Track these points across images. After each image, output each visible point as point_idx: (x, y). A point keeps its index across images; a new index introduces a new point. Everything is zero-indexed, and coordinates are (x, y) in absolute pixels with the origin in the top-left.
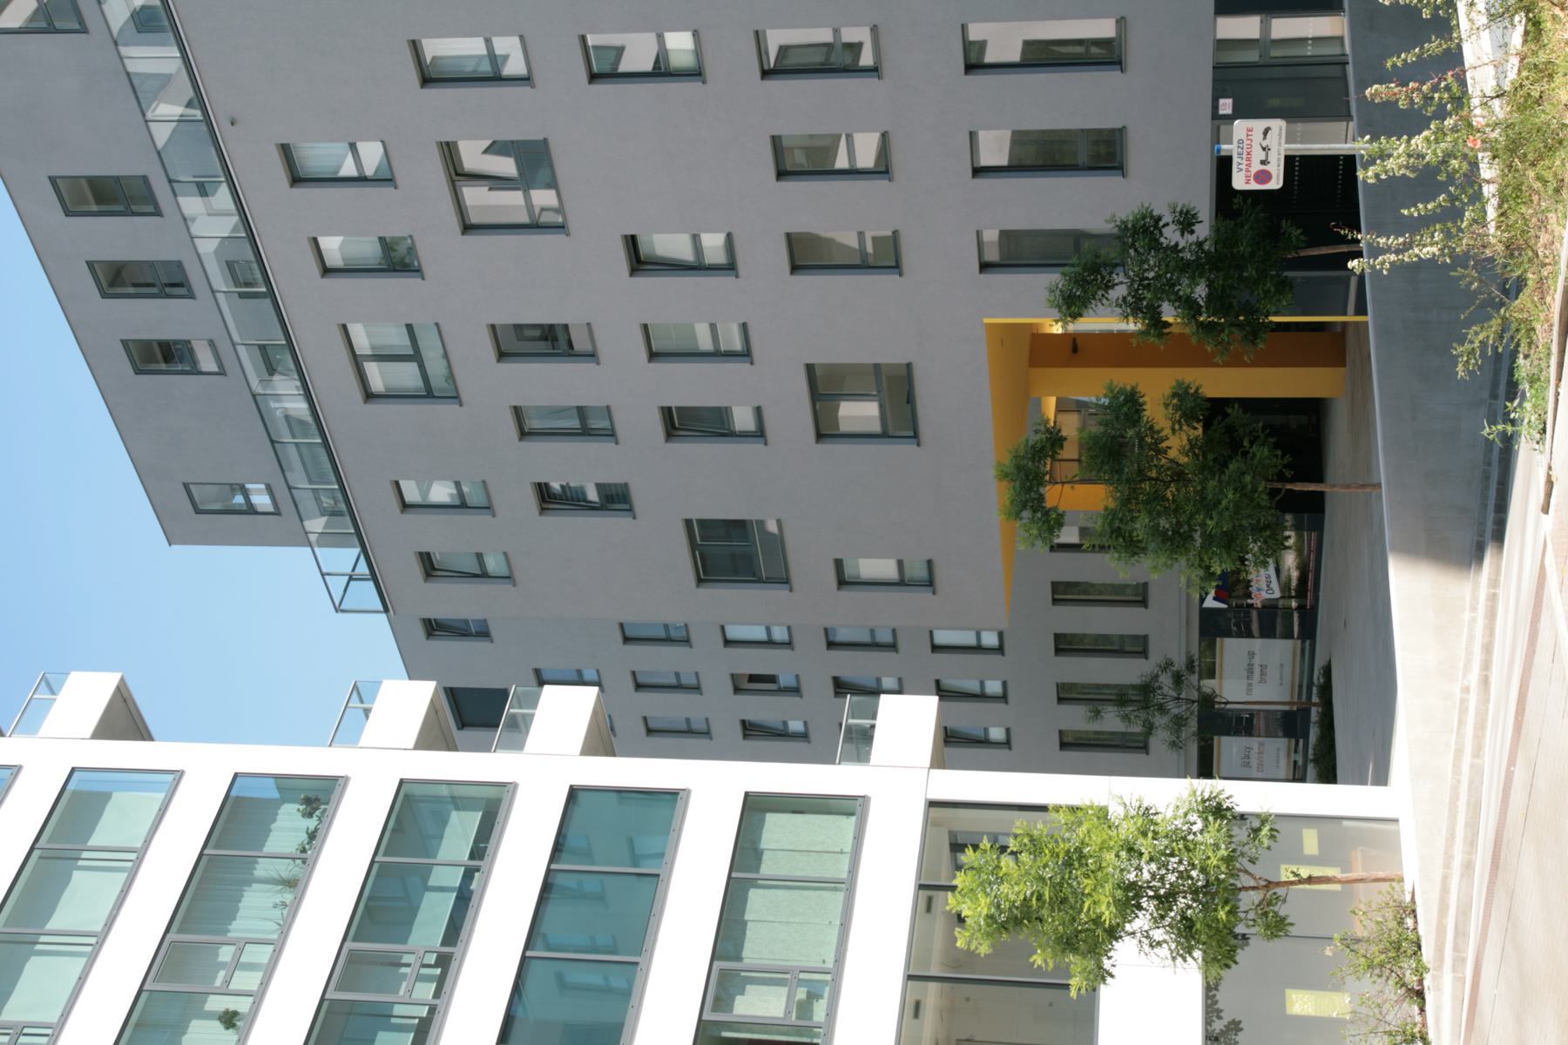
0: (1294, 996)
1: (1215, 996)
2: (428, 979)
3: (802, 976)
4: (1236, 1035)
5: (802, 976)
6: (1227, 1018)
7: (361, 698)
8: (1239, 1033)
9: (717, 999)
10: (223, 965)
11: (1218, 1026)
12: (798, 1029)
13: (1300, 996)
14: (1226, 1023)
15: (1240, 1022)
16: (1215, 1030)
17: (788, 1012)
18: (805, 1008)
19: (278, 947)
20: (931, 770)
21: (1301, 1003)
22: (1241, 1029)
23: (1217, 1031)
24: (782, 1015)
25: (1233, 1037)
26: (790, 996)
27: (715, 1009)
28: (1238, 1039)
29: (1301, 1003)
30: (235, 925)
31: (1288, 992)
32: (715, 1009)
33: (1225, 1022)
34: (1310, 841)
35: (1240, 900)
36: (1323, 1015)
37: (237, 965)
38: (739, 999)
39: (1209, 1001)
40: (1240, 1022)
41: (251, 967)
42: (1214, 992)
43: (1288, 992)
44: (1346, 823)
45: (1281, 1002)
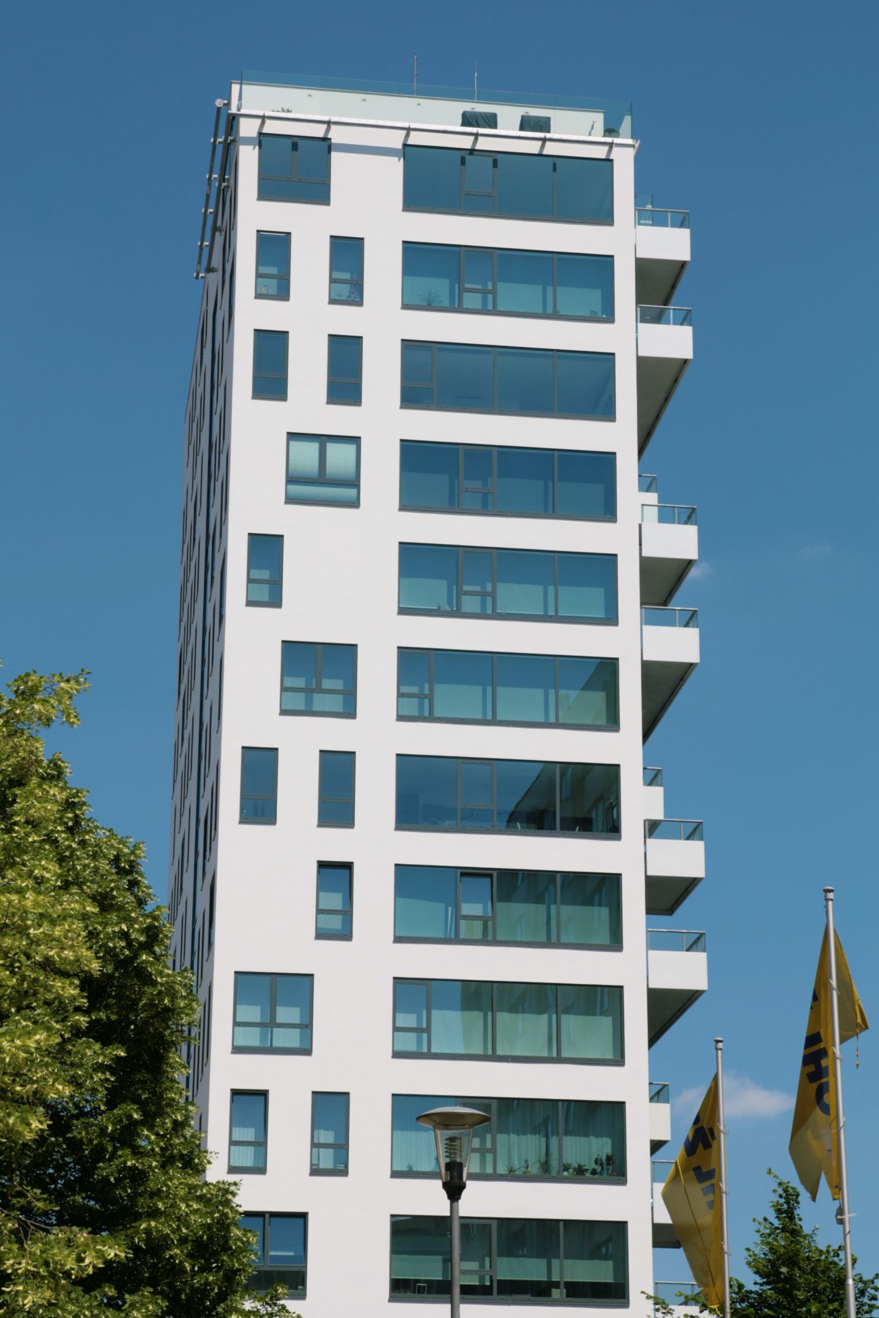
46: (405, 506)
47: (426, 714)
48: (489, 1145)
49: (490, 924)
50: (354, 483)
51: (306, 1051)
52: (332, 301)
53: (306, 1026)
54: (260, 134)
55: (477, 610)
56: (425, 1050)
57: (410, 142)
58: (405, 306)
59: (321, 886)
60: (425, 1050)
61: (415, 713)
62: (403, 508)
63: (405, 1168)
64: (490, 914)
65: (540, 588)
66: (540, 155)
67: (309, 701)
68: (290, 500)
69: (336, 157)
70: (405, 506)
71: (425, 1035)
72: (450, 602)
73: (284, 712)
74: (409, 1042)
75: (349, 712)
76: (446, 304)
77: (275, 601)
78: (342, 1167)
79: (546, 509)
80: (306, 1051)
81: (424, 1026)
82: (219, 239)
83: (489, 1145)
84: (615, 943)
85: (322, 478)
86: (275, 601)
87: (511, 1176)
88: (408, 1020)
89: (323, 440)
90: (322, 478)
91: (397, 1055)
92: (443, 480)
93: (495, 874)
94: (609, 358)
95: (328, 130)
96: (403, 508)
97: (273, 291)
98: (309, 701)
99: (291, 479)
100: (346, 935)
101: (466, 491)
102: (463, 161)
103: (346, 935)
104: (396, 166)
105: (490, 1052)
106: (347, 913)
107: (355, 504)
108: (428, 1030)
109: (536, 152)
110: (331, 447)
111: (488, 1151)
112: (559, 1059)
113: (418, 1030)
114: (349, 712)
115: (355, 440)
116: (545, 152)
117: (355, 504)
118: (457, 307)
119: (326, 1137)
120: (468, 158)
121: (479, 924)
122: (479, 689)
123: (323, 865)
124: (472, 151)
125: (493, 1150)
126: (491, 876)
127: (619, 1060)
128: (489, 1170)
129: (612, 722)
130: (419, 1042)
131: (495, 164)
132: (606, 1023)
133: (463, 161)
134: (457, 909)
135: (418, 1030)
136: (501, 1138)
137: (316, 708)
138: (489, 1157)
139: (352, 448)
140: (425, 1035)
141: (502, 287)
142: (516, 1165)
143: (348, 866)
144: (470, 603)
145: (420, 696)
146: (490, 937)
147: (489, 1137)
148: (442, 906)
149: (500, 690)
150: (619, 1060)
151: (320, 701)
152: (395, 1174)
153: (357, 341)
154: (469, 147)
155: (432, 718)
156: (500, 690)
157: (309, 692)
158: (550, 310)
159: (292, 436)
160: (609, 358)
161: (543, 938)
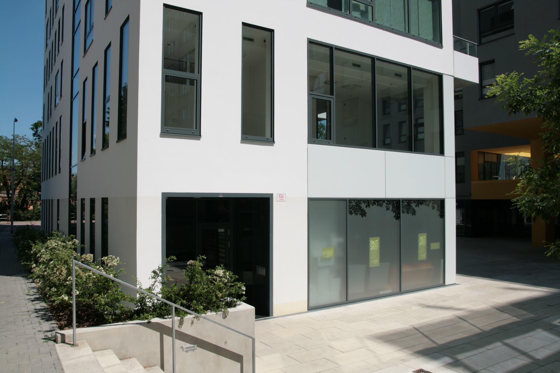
0: (377, 241)
1: (375, 204)
3: (370, 8)
4: (360, 214)
5: (370, 8)
6: (367, 210)
8: (361, 216)
11: (363, 206)
13: (377, 244)
14: (364, 210)
15: (365, 216)
16: (362, 204)
20: (452, 78)
21: (374, 244)
22: (362, 217)
23: (361, 205)
25: (359, 213)
28: (358, 215)
29: (374, 244)
31: (378, 238)
33: (365, 209)
34: (435, 246)
35: (393, 213)
36: (370, 254)
39: (421, 201)
40: (365, 216)
42: (377, 204)
43: (378, 238)
44: (442, 261)
45: (374, 236)
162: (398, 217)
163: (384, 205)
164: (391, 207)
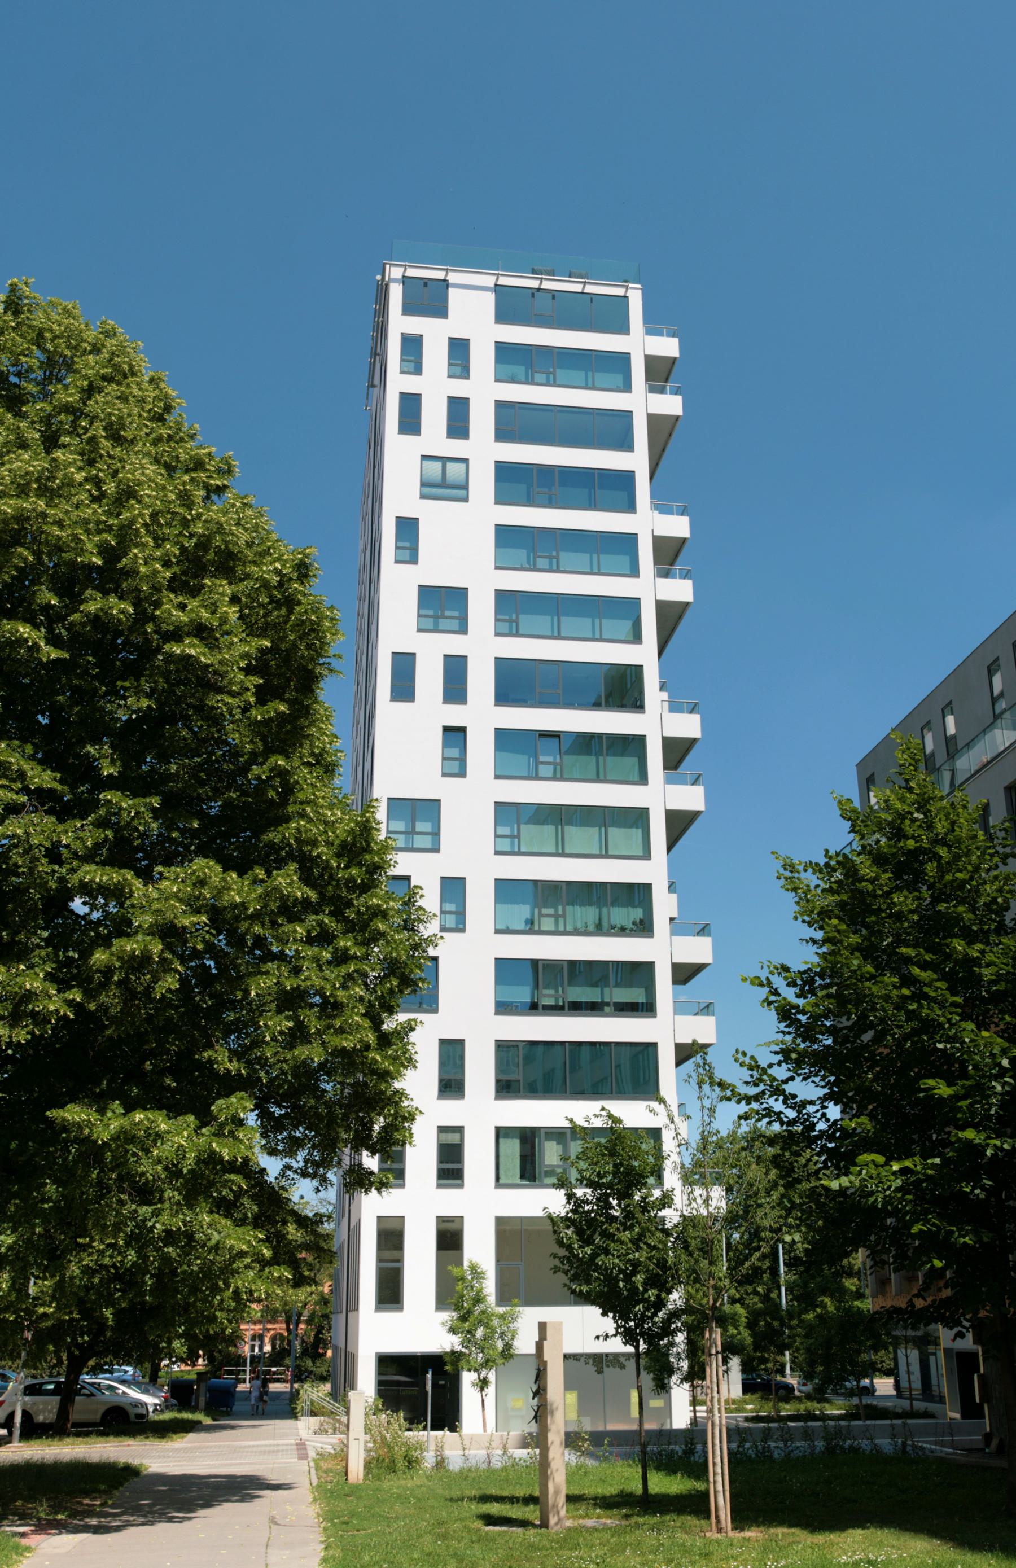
2: (557, 1000)
7: (703, 931)
9: (552, 1133)
10: (556, 910)
12: (540, 1172)
17: (547, 1166)
18: (550, 1173)
19: (565, 933)
24: (547, 1162)
26: (558, 1166)
27: (546, 1133)
30: (578, 909)
32: (546, 1133)
37: (556, 917)
38: (555, 1143)
41: (557, 923)
46: (498, 501)
47: (514, 632)
48: (560, 912)
49: (558, 767)
50: (465, 487)
51: (437, 850)
52: (450, 376)
53: (436, 834)
54: (404, 277)
55: (547, 567)
56: (516, 850)
57: (499, 283)
58: (497, 380)
59: (446, 744)
60: (516, 850)
61: (507, 631)
62: (497, 502)
63: (504, 928)
64: (558, 760)
65: (588, 556)
66: (582, 293)
67: (436, 624)
68: (423, 496)
69: (452, 292)
70: (498, 501)
71: (516, 840)
72: (528, 562)
73: (419, 630)
74: (506, 845)
75: (463, 630)
76: (523, 379)
77: (414, 560)
78: (461, 926)
79: (590, 505)
80: (437, 850)
81: (516, 833)
82: (378, 358)
83: (560, 912)
84: (643, 779)
85: (443, 483)
86: (414, 560)
87: (576, 932)
88: (505, 831)
89: (444, 460)
90: (443, 483)
91: (497, 853)
92: (523, 487)
93: (562, 735)
94: (629, 414)
95: (446, 275)
96: (497, 502)
97: (412, 370)
98: (436, 624)
99: (423, 484)
100: (462, 773)
101: (538, 493)
102: (533, 295)
103: (462, 773)
104: (490, 298)
105: (560, 851)
106: (462, 760)
107: (466, 499)
108: (518, 837)
109: (580, 290)
110: (450, 466)
111: (560, 916)
112: (607, 856)
113: (511, 837)
114: (463, 630)
115: (466, 461)
116: (586, 291)
117: (466, 499)
118: (530, 381)
119: (450, 907)
120: (536, 294)
121: (551, 767)
122: (549, 618)
123: (447, 729)
124: (539, 290)
125: (564, 916)
126: (559, 736)
127: (647, 855)
128: (561, 928)
129: (636, 637)
130: (512, 844)
131: (554, 297)
132: (637, 833)
133: (533, 295)
134: (536, 758)
135: (511, 837)
136: (569, 909)
137: (440, 628)
138: (561, 921)
139: (463, 466)
140: (516, 840)
141: (559, 371)
142: (579, 925)
143: (463, 730)
144: (541, 563)
145: (510, 621)
146: (558, 775)
147: (560, 908)
148: (526, 757)
149: (563, 619)
150: (647, 855)
151: (443, 623)
152: (498, 931)
153: (466, 400)
154: (537, 286)
155: (518, 635)
156: (563, 619)
157: (436, 617)
158: (590, 385)
159: (424, 457)
160: (629, 414)
161: (594, 777)
162: (600, 1372)
163: (582, 1359)
164: (591, 1361)
